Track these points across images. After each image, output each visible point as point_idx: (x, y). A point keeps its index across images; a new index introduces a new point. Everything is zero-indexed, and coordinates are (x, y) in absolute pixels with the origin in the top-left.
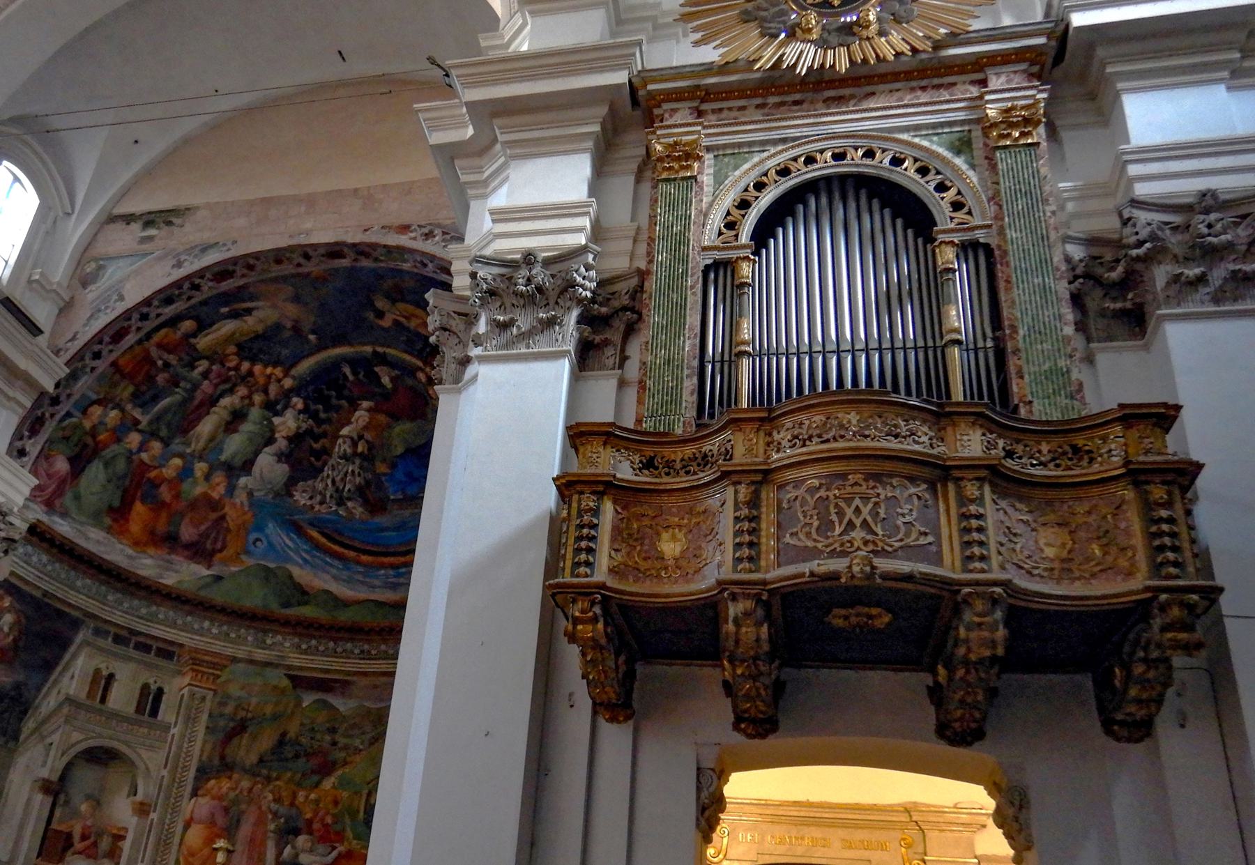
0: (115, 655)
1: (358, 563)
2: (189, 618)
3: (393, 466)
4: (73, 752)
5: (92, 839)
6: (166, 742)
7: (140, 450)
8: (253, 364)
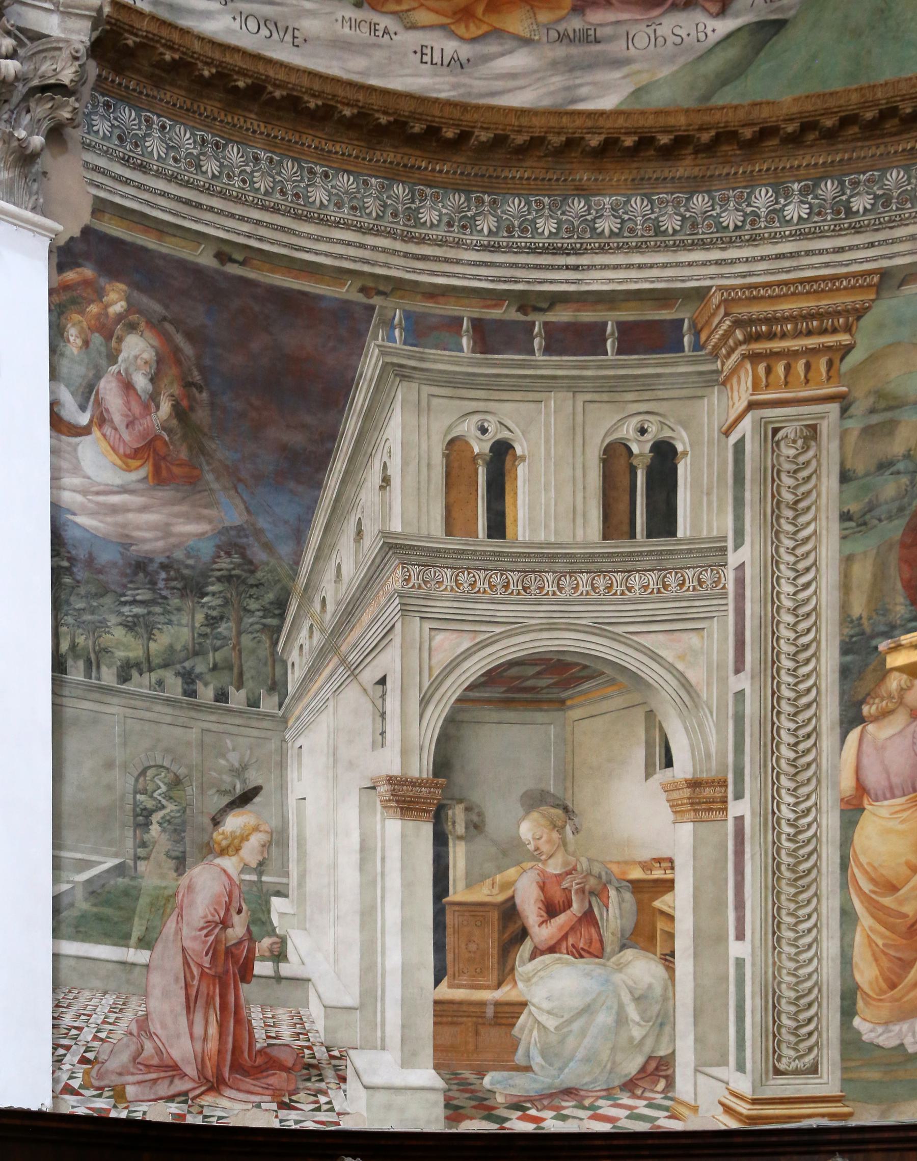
4: (453, 688)
5: (577, 908)
6: (724, 596)
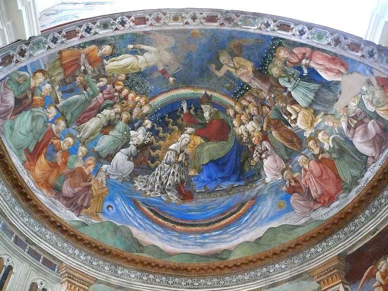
0: (14, 251)
1: (174, 230)
2: (65, 244)
3: (200, 171)
7: (52, 122)
8: (130, 92)
